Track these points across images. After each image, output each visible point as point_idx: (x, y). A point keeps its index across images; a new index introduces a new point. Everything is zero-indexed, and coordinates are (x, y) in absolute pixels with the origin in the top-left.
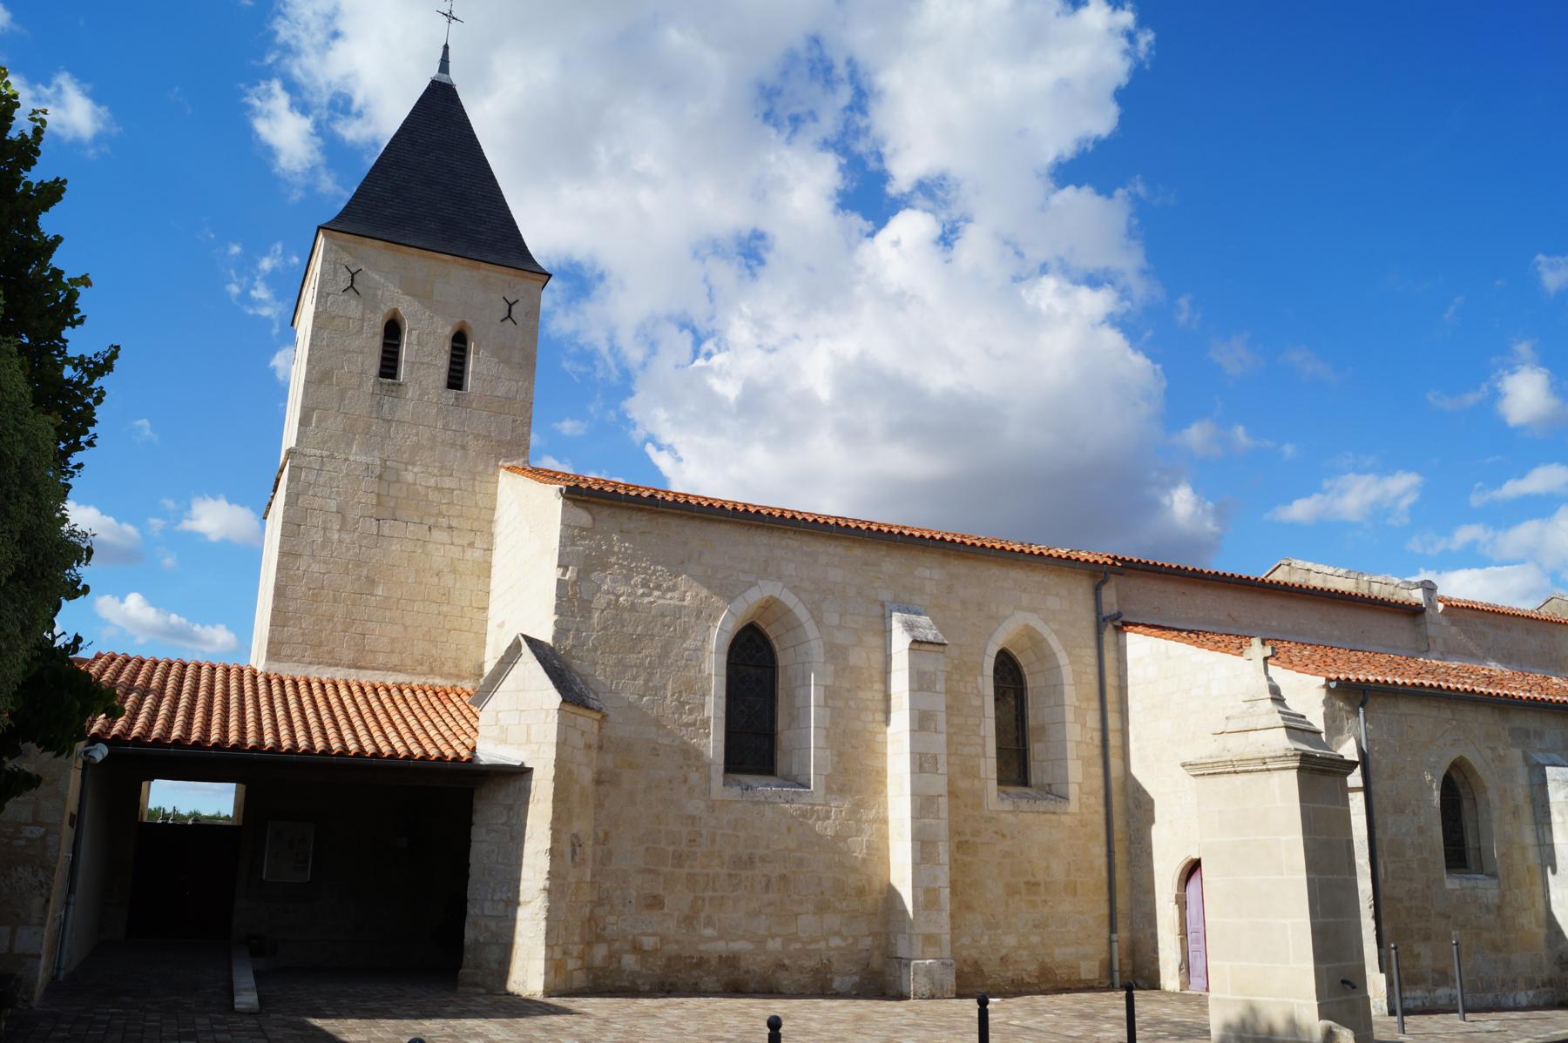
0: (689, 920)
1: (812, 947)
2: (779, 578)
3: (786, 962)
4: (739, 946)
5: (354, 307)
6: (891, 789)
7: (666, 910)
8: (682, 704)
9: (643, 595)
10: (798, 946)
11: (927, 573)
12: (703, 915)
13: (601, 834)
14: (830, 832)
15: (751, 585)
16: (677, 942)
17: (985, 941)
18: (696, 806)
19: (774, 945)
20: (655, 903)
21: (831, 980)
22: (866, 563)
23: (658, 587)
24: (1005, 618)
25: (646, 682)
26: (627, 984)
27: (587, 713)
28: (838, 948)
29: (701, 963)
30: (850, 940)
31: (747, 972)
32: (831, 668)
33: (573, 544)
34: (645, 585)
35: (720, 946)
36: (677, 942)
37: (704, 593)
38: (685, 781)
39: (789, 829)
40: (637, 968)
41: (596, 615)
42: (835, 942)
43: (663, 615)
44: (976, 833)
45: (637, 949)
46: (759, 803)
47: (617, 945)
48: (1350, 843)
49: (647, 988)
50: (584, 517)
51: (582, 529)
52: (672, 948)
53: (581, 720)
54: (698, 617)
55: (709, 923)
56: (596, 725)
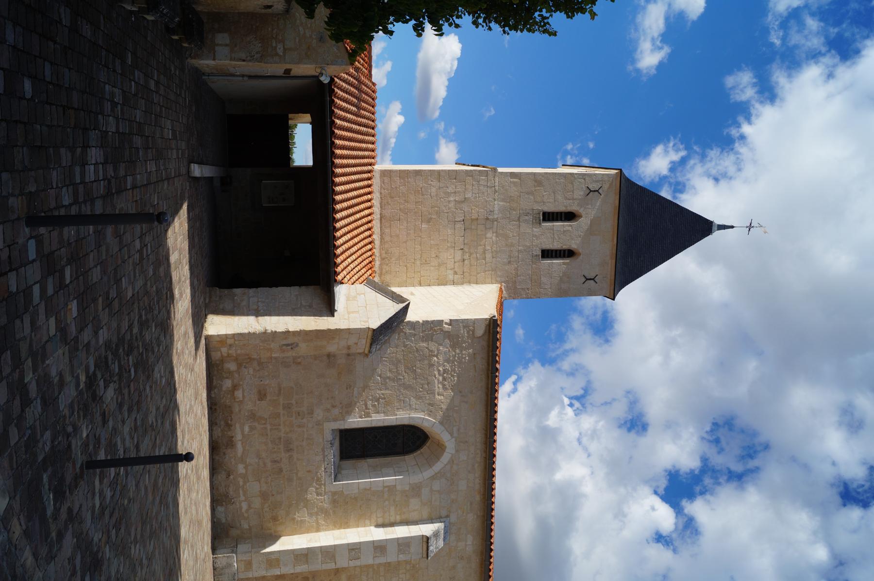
0: (253, 416)
1: (241, 492)
2: (457, 451)
3: (231, 477)
4: (239, 446)
7: (258, 402)
8: (378, 400)
9: (439, 371)
10: (241, 483)
11: (469, 542)
12: (256, 424)
13: (299, 360)
14: (309, 496)
15: (451, 434)
16: (240, 411)
18: (319, 414)
19: (241, 469)
20: (262, 395)
22: (471, 504)
23: (444, 379)
25: (389, 378)
28: (241, 508)
29: (229, 426)
30: (246, 515)
31: (224, 454)
33: (464, 327)
35: (239, 437)
36: (240, 411)
37: (444, 407)
38: (334, 407)
39: (309, 471)
40: (224, 389)
41: (425, 345)
42: (245, 506)
43: (428, 384)
45: (235, 387)
46: (323, 450)
49: (213, 396)
50: (480, 331)
51: (473, 331)
52: (236, 409)
53: (364, 341)
54: (430, 404)
55: (252, 428)
56: (361, 351)
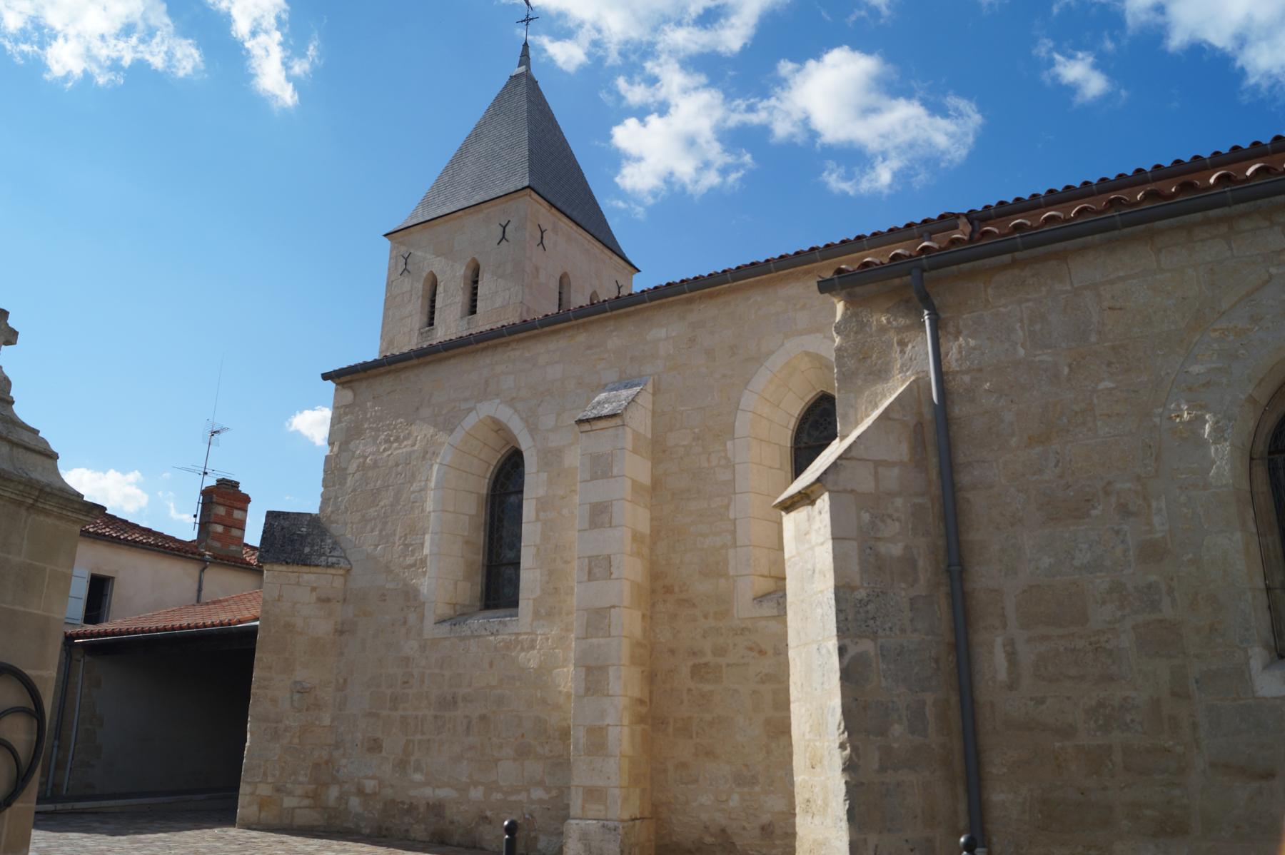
0: (402, 765)
1: (513, 798)
2: (497, 395)
3: (489, 813)
4: (443, 793)
5: (406, 284)
6: (825, 587)
7: (384, 754)
8: (407, 546)
9: (385, 450)
10: (499, 796)
11: (662, 333)
12: (413, 759)
13: (341, 681)
14: (533, 664)
15: (470, 410)
16: (392, 786)
17: (735, 801)
18: (410, 647)
19: (476, 794)
20: (375, 746)
21: (536, 838)
22: (590, 348)
23: (397, 440)
24: (770, 353)
25: (381, 531)
26: (351, 825)
27: (313, 569)
28: (541, 801)
29: (411, 809)
30: (554, 793)
31: (452, 822)
32: (544, 476)
33: (340, 422)
34: (387, 441)
35: (428, 792)
36: (392, 786)
37: (432, 431)
38: (405, 622)
39: (491, 665)
40: (359, 810)
41: (349, 479)
42: (538, 794)
43: (397, 465)
44: (720, 651)
45: (360, 792)
46: (463, 638)
47: (346, 787)
48: (779, 727)
49: (367, 831)
50: (348, 395)
51: (346, 406)
52: (388, 792)
53: (306, 577)
54: (424, 458)
55: (418, 769)
56: (341, 580)
